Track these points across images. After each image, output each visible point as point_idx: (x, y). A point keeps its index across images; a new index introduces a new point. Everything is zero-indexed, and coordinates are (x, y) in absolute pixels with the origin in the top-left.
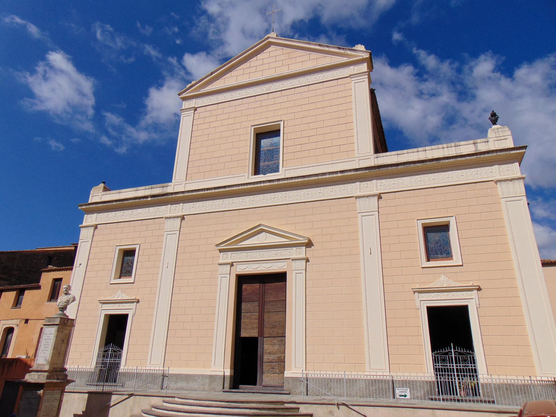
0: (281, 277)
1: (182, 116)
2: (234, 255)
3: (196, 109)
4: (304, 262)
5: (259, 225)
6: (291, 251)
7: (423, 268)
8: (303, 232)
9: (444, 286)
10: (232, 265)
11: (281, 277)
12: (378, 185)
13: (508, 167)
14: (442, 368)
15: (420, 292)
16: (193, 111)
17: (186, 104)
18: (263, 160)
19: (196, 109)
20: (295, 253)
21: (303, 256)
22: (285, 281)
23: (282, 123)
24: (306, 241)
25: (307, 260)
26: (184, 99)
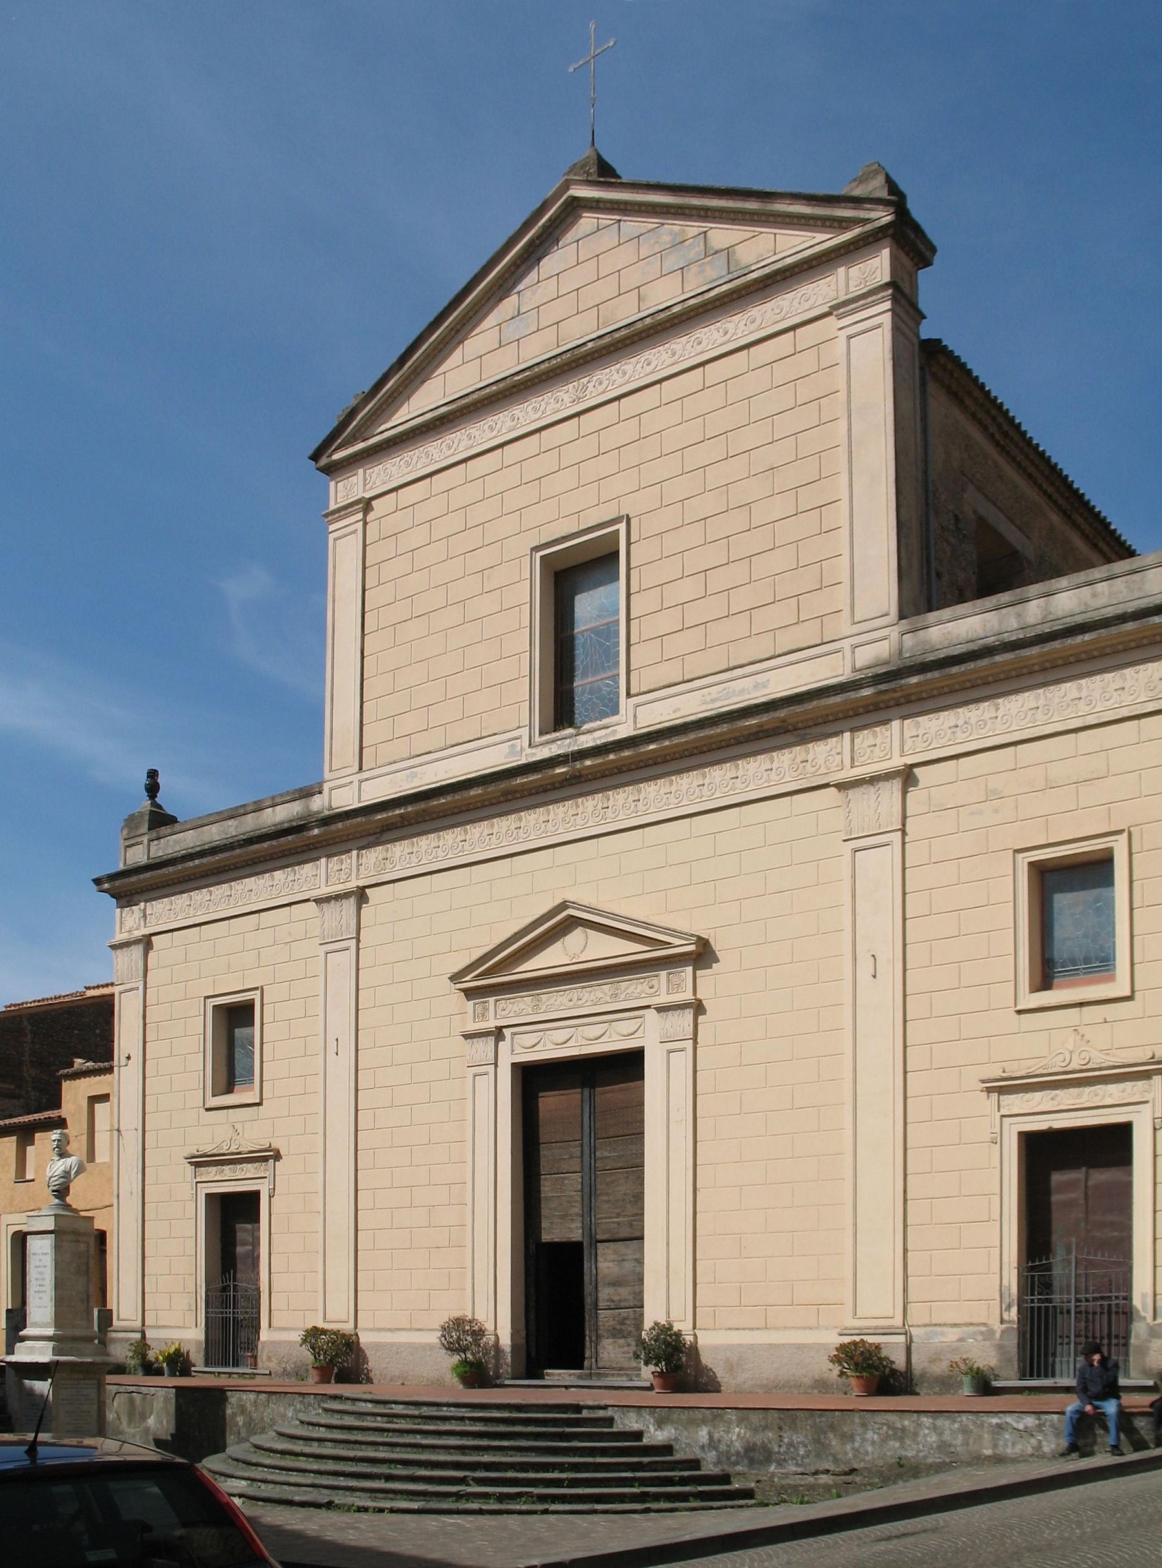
0: (628, 1065)
1: (331, 537)
2: (502, 1004)
3: (366, 505)
4: (689, 1014)
5: (563, 906)
6: (655, 982)
7: (1019, 1012)
8: (681, 919)
9: (1074, 1065)
10: (498, 1034)
11: (628, 1065)
12: (907, 734)
13: (1037, 698)
14: (1039, 1308)
15: (1002, 1091)
16: (360, 516)
17: (343, 490)
18: (564, 678)
19: (366, 505)
20: (663, 987)
21: (687, 996)
22: (641, 1076)
23: (622, 527)
24: (692, 948)
25: (698, 1008)
26: (332, 470)
